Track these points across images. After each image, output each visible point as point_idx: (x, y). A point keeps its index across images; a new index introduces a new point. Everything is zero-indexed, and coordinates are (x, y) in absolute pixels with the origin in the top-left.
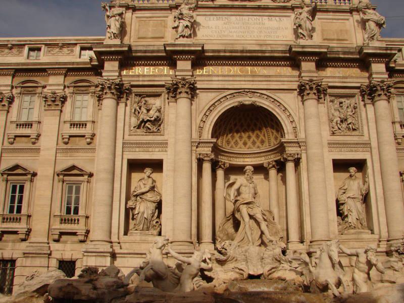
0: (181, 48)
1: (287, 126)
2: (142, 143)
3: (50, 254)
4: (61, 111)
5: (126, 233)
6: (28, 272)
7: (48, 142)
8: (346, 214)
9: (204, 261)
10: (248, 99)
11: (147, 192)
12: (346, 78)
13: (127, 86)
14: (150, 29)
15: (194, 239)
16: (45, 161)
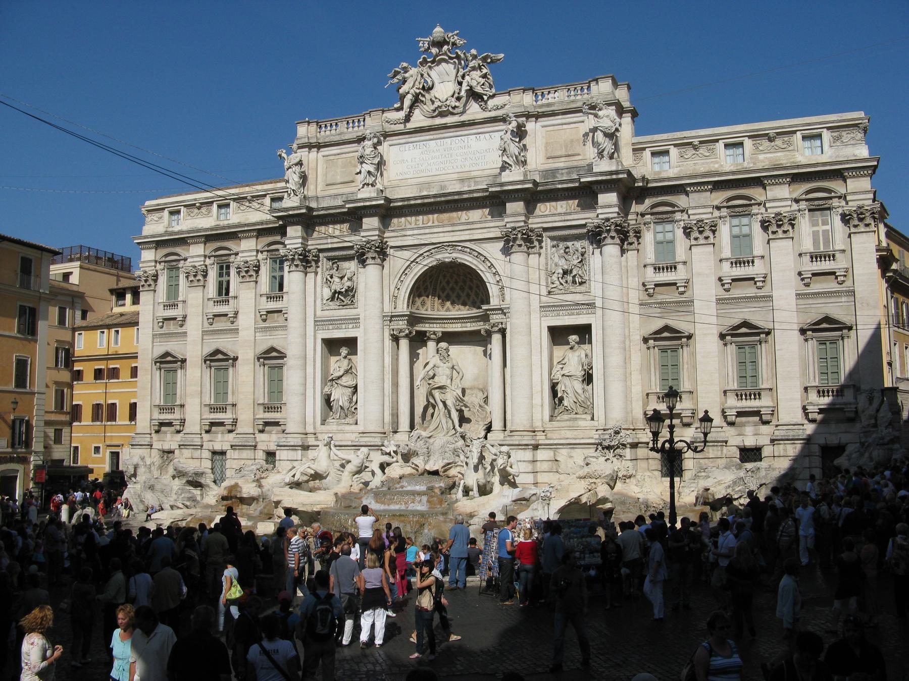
0: (362, 204)
1: (493, 290)
2: (334, 320)
3: (255, 446)
4: (256, 282)
5: (323, 422)
6: (236, 465)
7: (247, 321)
8: (559, 395)
9: (389, 454)
10: (448, 255)
11: (341, 376)
12: (570, 214)
13: (314, 252)
14: (338, 171)
15: (388, 428)
16: (246, 342)
